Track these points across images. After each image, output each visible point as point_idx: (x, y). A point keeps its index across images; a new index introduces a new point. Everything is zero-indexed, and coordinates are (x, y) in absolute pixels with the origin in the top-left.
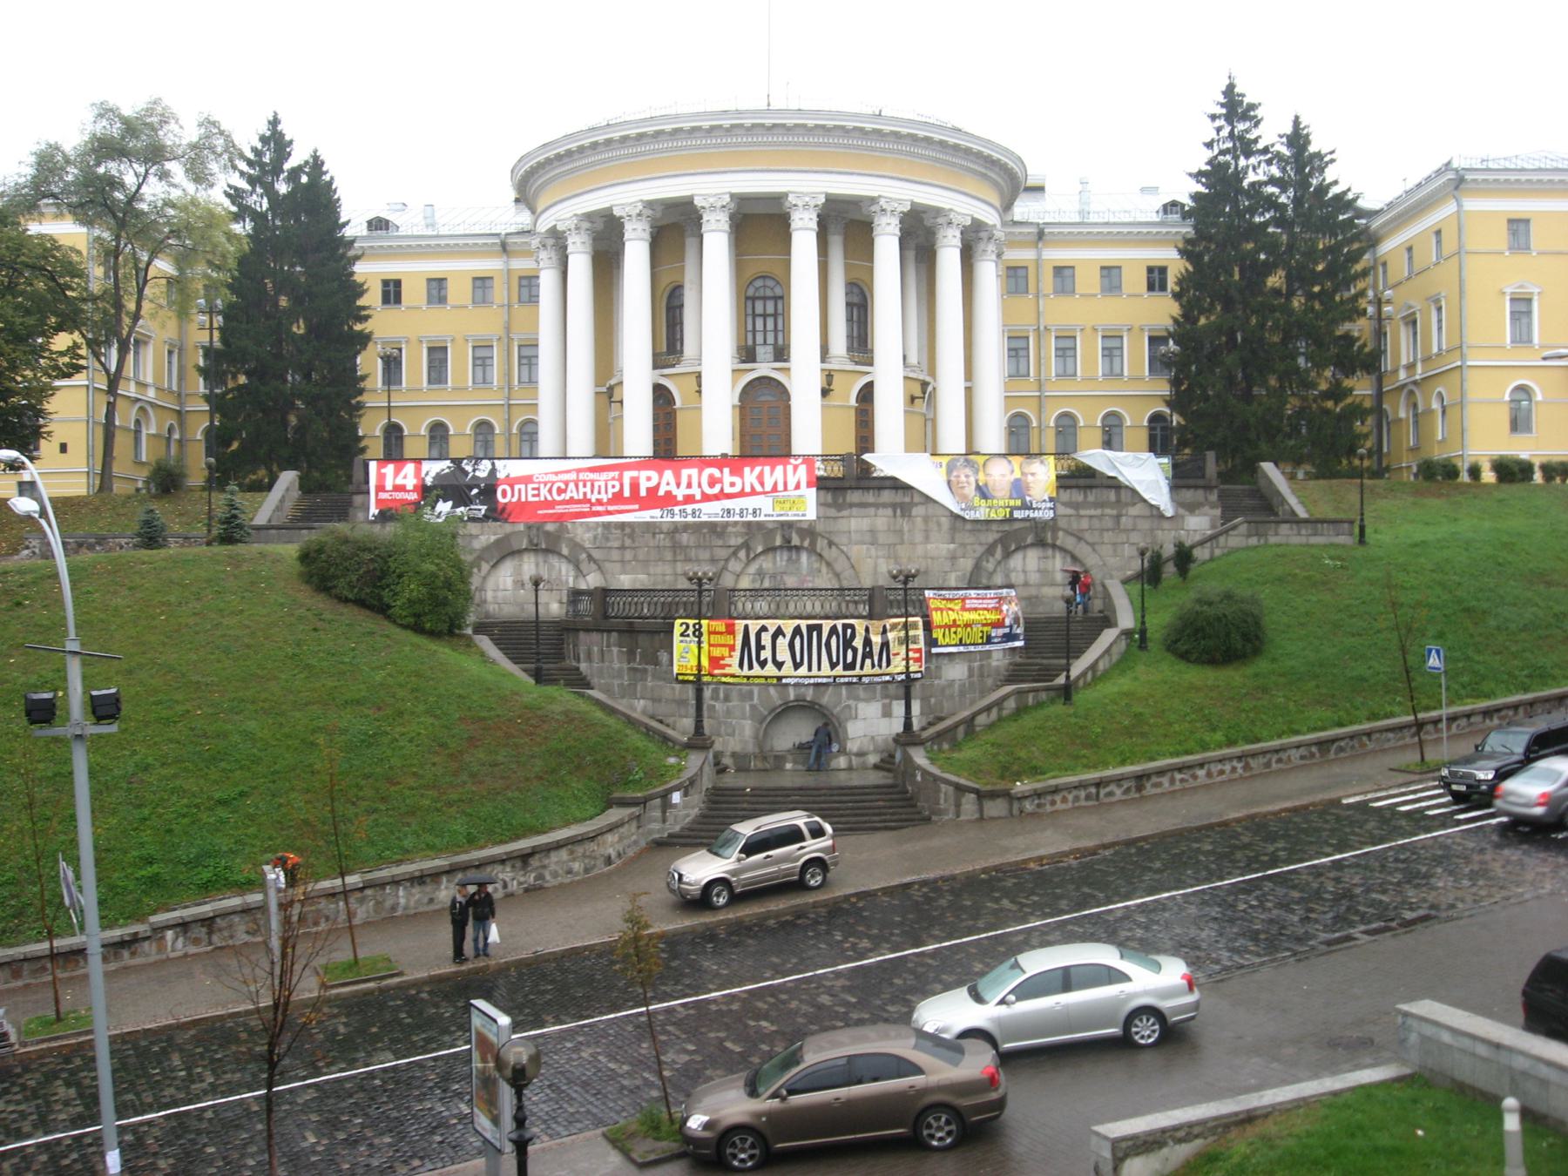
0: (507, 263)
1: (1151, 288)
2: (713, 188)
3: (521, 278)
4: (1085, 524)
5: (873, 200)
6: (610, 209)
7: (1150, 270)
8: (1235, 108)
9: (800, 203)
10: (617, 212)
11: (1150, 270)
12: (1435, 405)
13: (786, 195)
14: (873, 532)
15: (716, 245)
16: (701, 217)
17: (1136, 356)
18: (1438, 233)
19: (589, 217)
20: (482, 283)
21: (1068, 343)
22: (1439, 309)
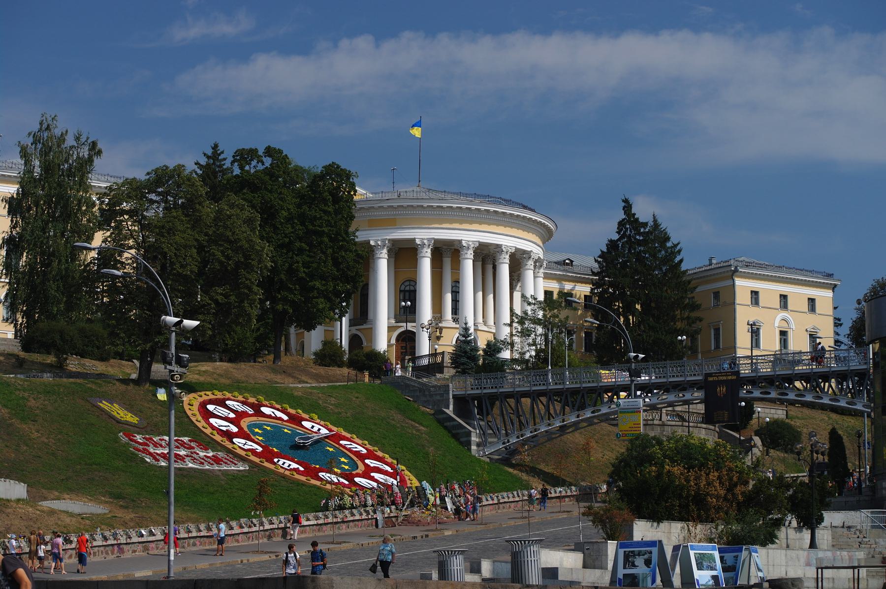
5: (524, 252)
6: (414, 240)
8: (630, 222)
10: (418, 242)
13: (499, 246)
15: (468, 266)
18: (717, 295)
22: (717, 331)
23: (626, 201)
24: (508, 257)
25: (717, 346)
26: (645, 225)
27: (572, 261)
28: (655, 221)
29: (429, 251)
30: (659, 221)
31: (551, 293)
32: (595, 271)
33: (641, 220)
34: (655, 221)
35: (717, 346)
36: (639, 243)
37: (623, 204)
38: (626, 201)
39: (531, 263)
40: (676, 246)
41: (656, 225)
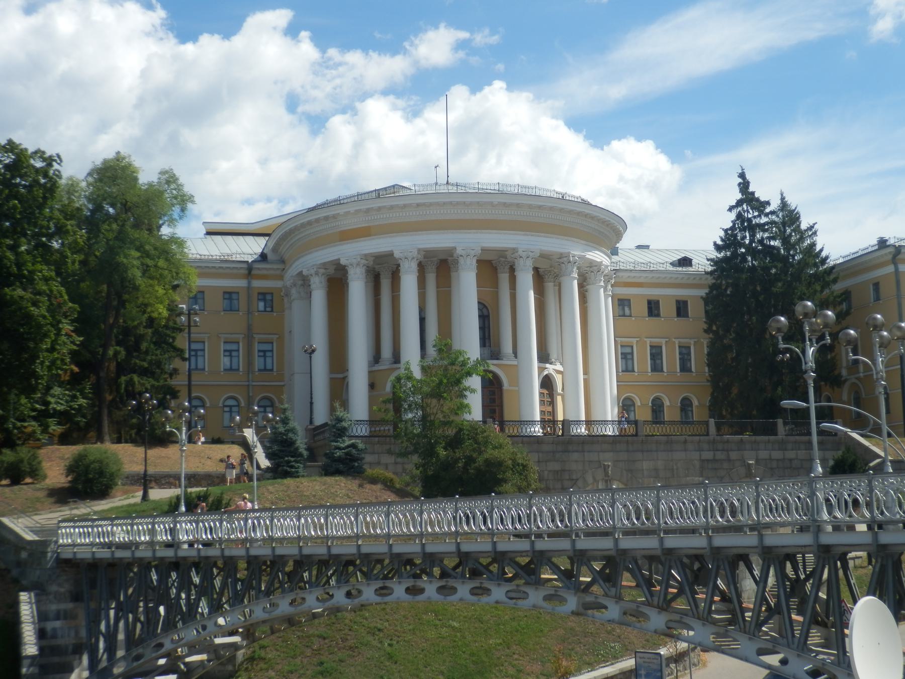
0: (249, 283)
1: (679, 314)
3: (259, 294)
4: (774, 464)
7: (678, 302)
9: (524, 255)
10: (397, 254)
11: (678, 302)
13: (515, 250)
16: (456, 262)
18: (876, 285)
19: (366, 256)
20: (229, 295)
21: (628, 350)
23: (742, 175)
26: (768, 203)
28: (783, 199)
29: (414, 266)
32: (710, 269)
33: (762, 199)
34: (783, 199)
36: (761, 227)
37: (740, 180)
38: (742, 175)
40: (811, 228)
41: (784, 205)
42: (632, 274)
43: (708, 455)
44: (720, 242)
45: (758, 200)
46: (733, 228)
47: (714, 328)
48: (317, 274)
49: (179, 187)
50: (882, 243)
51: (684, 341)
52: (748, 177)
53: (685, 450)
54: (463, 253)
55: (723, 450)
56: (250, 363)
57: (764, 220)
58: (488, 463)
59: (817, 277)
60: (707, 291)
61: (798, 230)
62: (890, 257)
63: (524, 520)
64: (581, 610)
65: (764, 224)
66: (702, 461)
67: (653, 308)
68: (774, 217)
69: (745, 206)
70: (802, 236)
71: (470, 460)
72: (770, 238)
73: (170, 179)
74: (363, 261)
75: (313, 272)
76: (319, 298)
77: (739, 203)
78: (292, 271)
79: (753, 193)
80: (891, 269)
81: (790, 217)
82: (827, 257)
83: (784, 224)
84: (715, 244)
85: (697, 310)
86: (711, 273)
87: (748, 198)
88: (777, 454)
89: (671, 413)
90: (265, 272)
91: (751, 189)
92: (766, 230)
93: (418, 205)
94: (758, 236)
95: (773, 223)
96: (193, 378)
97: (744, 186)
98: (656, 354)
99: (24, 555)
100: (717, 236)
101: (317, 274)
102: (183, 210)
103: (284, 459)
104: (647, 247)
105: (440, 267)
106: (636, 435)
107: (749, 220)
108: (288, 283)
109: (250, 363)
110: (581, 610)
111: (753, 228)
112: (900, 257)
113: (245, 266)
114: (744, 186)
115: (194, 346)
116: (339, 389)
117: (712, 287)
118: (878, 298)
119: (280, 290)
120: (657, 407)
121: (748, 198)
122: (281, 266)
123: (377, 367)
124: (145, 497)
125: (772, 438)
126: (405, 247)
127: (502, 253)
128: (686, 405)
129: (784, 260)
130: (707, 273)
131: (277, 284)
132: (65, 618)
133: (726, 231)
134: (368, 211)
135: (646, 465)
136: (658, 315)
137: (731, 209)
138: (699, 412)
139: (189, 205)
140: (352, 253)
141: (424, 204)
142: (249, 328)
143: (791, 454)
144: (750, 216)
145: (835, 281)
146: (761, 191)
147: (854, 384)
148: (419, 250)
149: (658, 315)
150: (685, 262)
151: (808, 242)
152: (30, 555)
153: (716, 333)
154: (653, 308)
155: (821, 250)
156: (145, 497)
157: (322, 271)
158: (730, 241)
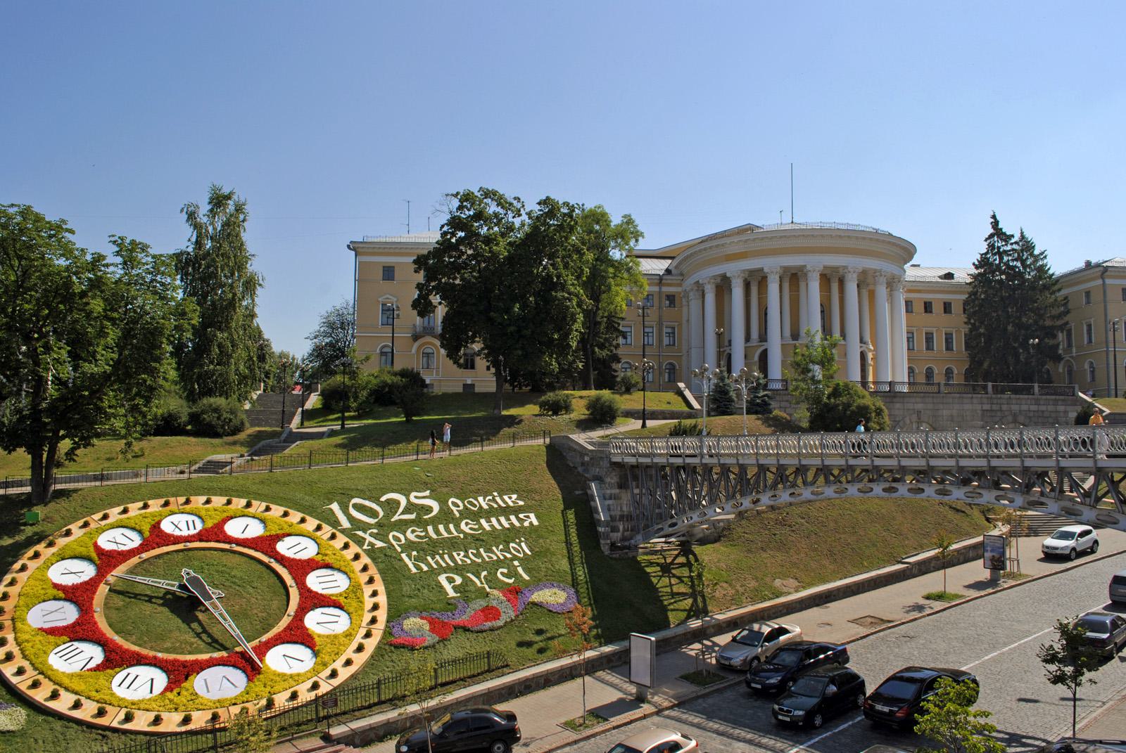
1: (945, 312)
2: (815, 263)
4: (1032, 414)
6: (762, 270)
9: (852, 270)
10: (766, 270)
12: (1087, 366)
13: (845, 267)
14: (952, 416)
16: (806, 275)
17: (939, 343)
18: (1088, 294)
22: (1089, 326)
24: (855, 276)
25: (1090, 341)
26: (1013, 236)
27: (953, 274)
28: (1022, 233)
30: (1027, 234)
31: (931, 303)
32: (969, 280)
33: (1008, 233)
34: (1022, 233)
35: (1090, 341)
36: (1005, 252)
37: (993, 220)
38: (994, 217)
39: (883, 280)
42: (914, 284)
43: (986, 407)
44: (977, 263)
45: (1005, 234)
46: (987, 253)
47: (972, 321)
48: (709, 283)
49: (635, 227)
50: (1088, 264)
51: (949, 330)
52: (998, 218)
53: (972, 403)
54: (811, 269)
55: (997, 404)
56: (660, 341)
57: (1009, 248)
58: (859, 407)
59: (1045, 287)
60: (967, 296)
61: (1032, 254)
62: (1100, 273)
63: (952, 446)
64: (1027, 506)
65: (1010, 251)
66: (983, 411)
67: (928, 307)
68: (1015, 247)
69: (996, 238)
70: (1036, 258)
71: (848, 405)
72: (1013, 260)
73: (629, 221)
74: (742, 275)
75: (706, 281)
76: (710, 298)
77: (991, 236)
78: (690, 282)
79: (1001, 229)
80: (1100, 282)
81: (1027, 246)
82: (1053, 274)
83: (1022, 251)
84: (974, 264)
85: (957, 308)
86: (970, 283)
87: (997, 232)
88: (1034, 408)
89: (939, 378)
90: (669, 282)
91: (1000, 226)
92: (1010, 255)
93: (781, 237)
94: (1005, 259)
95: (1013, 250)
96: (646, 350)
97: (995, 224)
98: (929, 338)
99: (587, 459)
100: (976, 258)
101: (709, 283)
102: (637, 241)
103: (721, 403)
104: (919, 266)
105: (794, 278)
106: (939, 392)
107: (999, 248)
108: (688, 289)
109: (660, 341)
110: (1027, 506)
111: (1001, 254)
112: (1107, 274)
113: (658, 277)
114: (995, 224)
115: (646, 330)
116: (726, 359)
117: (971, 294)
118: (1088, 302)
119: (680, 293)
120: (929, 374)
121: (997, 232)
122: (681, 278)
123: (748, 344)
124: (644, 425)
125: (1030, 396)
126: (772, 265)
127: (835, 269)
128: (949, 372)
129: (1021, 275)
130: (967, 284)
131: (679, 289)
132: (615, 499)
133: (982, 255)
134: (746, 241)
135: (945, 413)
136: (931, 312)
137: (986, 240)
138: (958, 379)
139: (640, 238)
140: (735, 270)
141: (785, 236)
142: (660, 318)
143: (1043, 408)
144: (999, 245)
145: (1059, 290)
146: (1006, 227)
147: (1068, 360)
148: (781, 267)
149: (931, 312)
150: (949, 276)
151: (1041, 263)
152: (591, 459)
153: (973, 325)
154: (928, 307)
155: (1049, 269)
156: (644, 425)
157: (713, 281)
158: (983, 262)
